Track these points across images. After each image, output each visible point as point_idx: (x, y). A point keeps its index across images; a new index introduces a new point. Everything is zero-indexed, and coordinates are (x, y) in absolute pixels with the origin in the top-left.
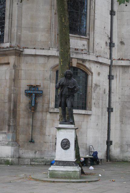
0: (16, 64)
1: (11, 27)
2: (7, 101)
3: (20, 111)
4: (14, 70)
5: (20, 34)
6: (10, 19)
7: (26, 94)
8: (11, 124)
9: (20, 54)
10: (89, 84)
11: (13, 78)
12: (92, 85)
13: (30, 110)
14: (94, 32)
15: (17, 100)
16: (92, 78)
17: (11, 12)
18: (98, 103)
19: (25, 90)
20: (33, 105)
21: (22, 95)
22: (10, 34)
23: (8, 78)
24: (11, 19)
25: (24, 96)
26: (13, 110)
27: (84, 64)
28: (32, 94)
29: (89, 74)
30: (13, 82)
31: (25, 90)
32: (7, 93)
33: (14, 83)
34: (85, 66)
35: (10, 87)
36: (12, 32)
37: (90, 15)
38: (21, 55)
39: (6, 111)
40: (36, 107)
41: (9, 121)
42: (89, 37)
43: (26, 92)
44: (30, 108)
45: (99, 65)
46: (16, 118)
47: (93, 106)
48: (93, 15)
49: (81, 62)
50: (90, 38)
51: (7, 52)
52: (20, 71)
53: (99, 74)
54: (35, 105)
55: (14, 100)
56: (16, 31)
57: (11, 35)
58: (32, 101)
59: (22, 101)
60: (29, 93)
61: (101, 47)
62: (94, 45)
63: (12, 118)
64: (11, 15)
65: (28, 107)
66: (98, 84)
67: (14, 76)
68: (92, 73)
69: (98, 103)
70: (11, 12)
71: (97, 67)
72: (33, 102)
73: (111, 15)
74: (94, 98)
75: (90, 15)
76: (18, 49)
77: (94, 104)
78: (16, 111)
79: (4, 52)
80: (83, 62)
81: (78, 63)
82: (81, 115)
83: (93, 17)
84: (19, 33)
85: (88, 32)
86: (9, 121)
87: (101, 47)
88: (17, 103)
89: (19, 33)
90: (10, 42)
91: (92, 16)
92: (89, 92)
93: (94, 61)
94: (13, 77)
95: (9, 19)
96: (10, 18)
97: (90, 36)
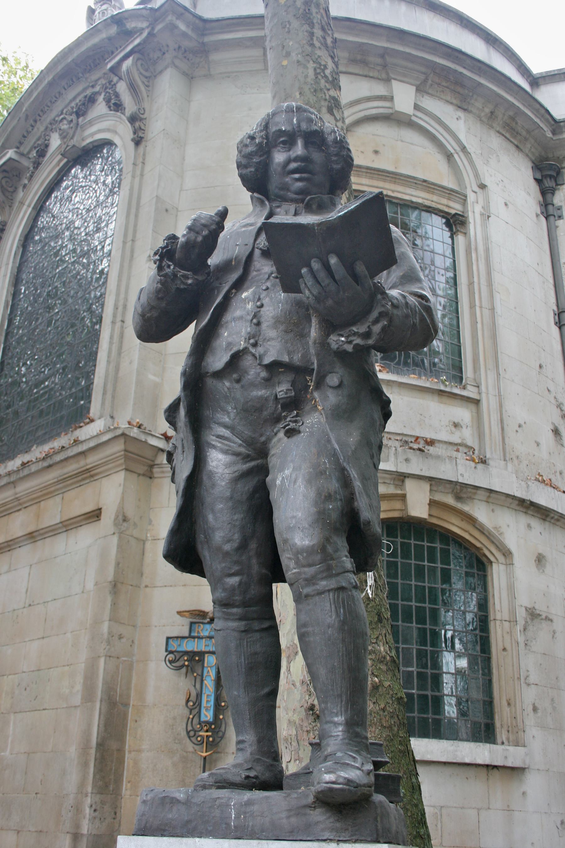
0: (130, 512)
1: (119, 353)
2: (77, 700)
3: (139, 751)
4: (115, 540)
5: (157, 380)
6: (118, 324)
7: (171, 657)
8: (85, 830)
9: (152, 466)
10: (497, 607)
11: (111, 577)
12: (513, 612)
13: (190, 747)
14: (498, 374)
15: (129, 689)
16: (510, 576)
17: (122, 296)
18: (554, 708)
19: (168, 638)
20: (208, 715)
21: (152, 666)
22: (110, 387)
23: (90, 585)
24: (123, 321)
25: (165, 670)
26: (100, 745)
27: (466, 508)
28: (201, 654)
29: (492, 558)
30: (109, 599)
31: (168, 638)
32: (84, 655)
33: (114, 604)
34: (471, 520)
35: (97, 622)
36: (121, 374)
37: (472, 306)
38: (155, 470)
39: (73, 751)
40: (223, 729)
41: (78, 809)
42: (480, 393)
43: (174, 645)
44: (191, 734)
45: (536, 523)
46: (117, 793)
47: (530, 720)
48: (485, 303)
49: (450, 500)
50: (484, 396)
51: (92, 460)
52: (148, 545)
53: (540, 560)
54: (216, 716)
55: (109, 689)
56: (135, 365)
57: (114, 390)
58: (199, 696)
59: (150, 697)
60: (186, 653)
61: (538, 444)
62: (503, 429)
63: (89, 789)
64: (120, 308)
65: (181, 729)
66: (541, 608)
67: (118, 564)
68: (507, 554)
69: (554, 708)
70: (122, 296)
71: (529, 526)
72: (204, 703)
73: (560, 328)
74: (532, 679)
75: (472, 306)
76: (135, 432)
77: (535, 709)
78: (121, 751)
79: (82, 463)
80: (458, 498)
81: (432, 503)
82: (471, 772)
83: (486, 312)
84: (151, 377)
85: (468, 372)
86: (78, 809)
87: (538, 444)
88: (127, 705)
89: (151, 377)
90: (112, 417)
91: (481, 307)
92: (504, 649)
93: (514, 497)
94: (110, 574)
95: (113, 323)
96: (119, 318)
97: (483, 388)
